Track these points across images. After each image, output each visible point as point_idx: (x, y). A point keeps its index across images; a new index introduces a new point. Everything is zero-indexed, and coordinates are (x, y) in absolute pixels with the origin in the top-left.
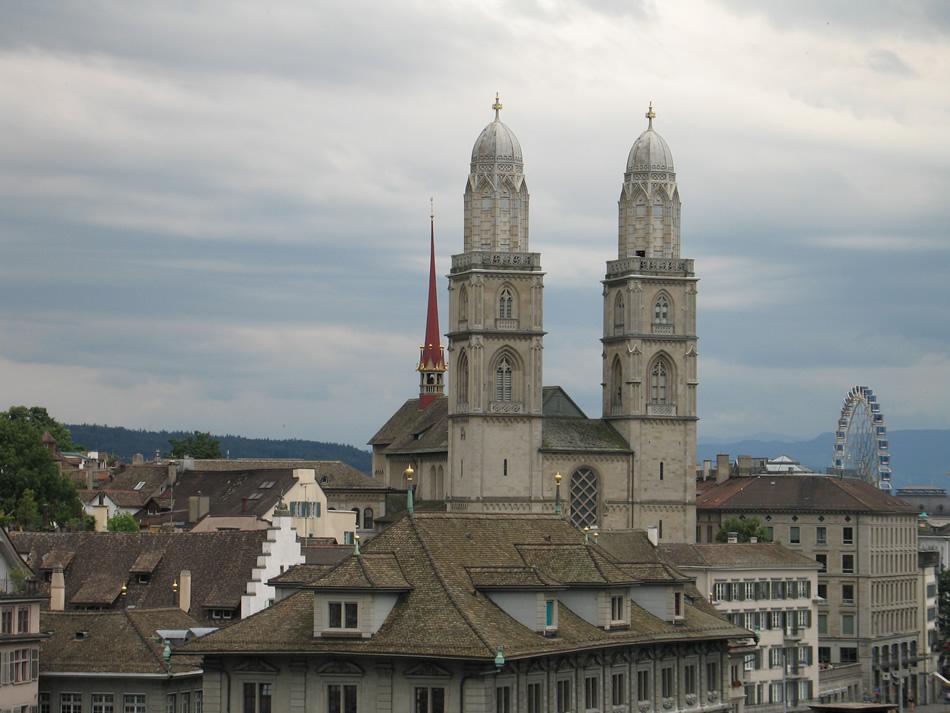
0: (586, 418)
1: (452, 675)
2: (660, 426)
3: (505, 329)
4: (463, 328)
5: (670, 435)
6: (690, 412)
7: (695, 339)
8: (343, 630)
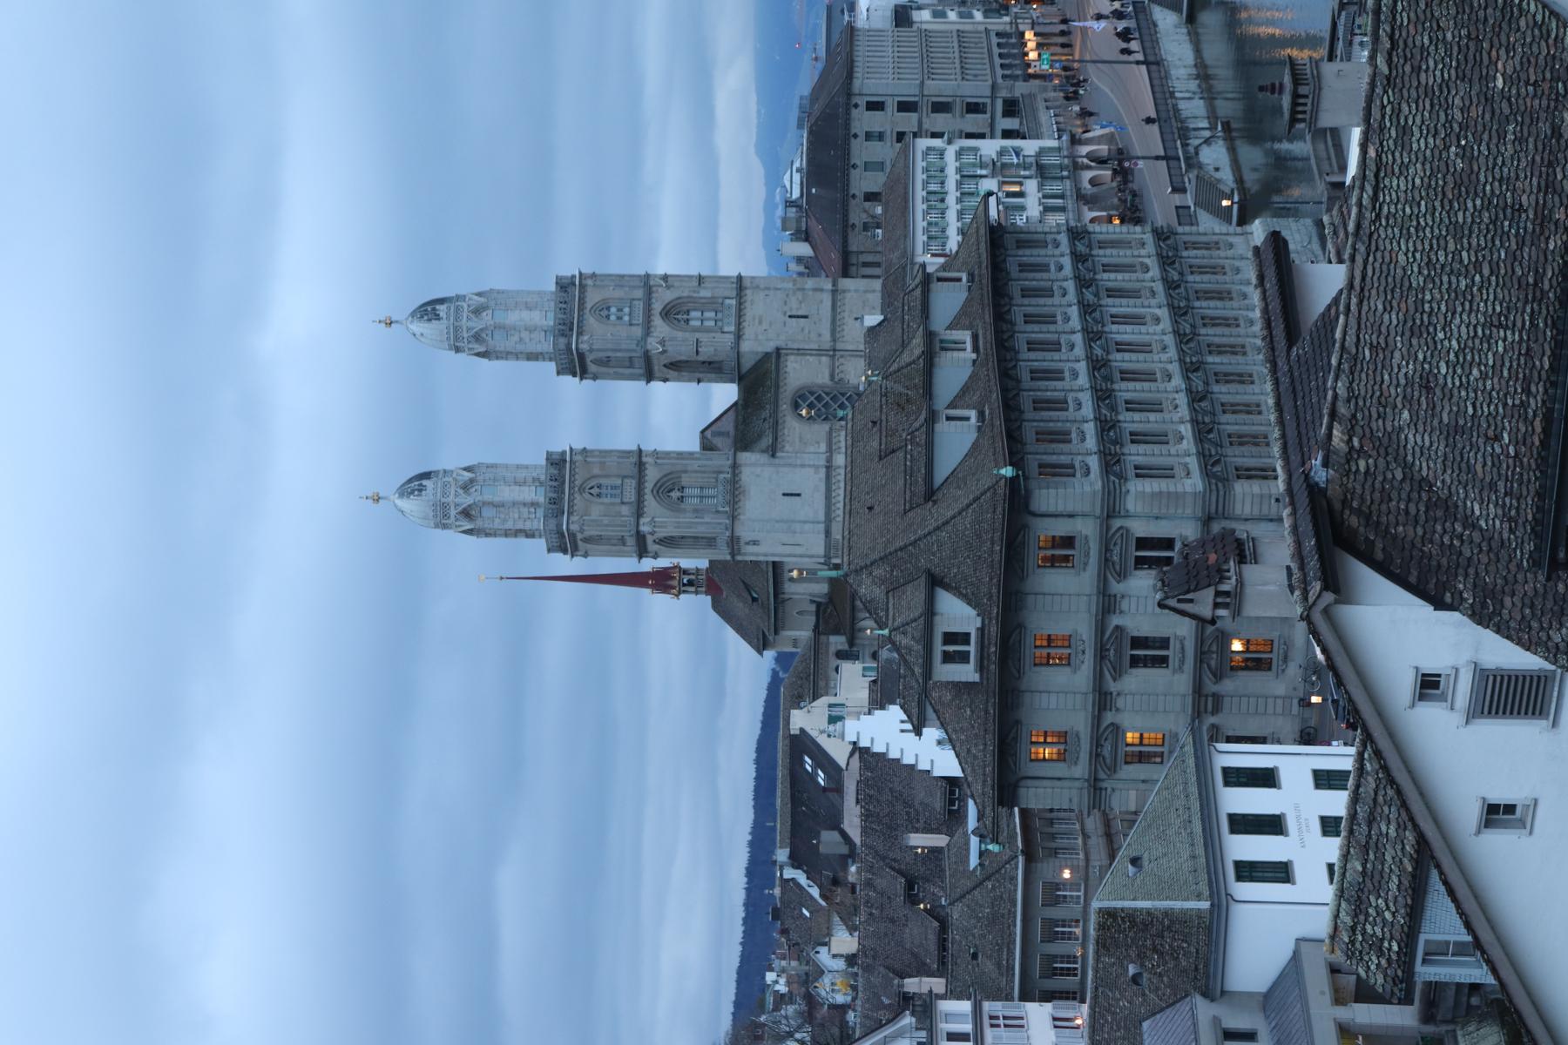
0: (735, 404)
1: (1025, 527)
4: (631, 541)
5: (757, 306)
8: (972, 648)
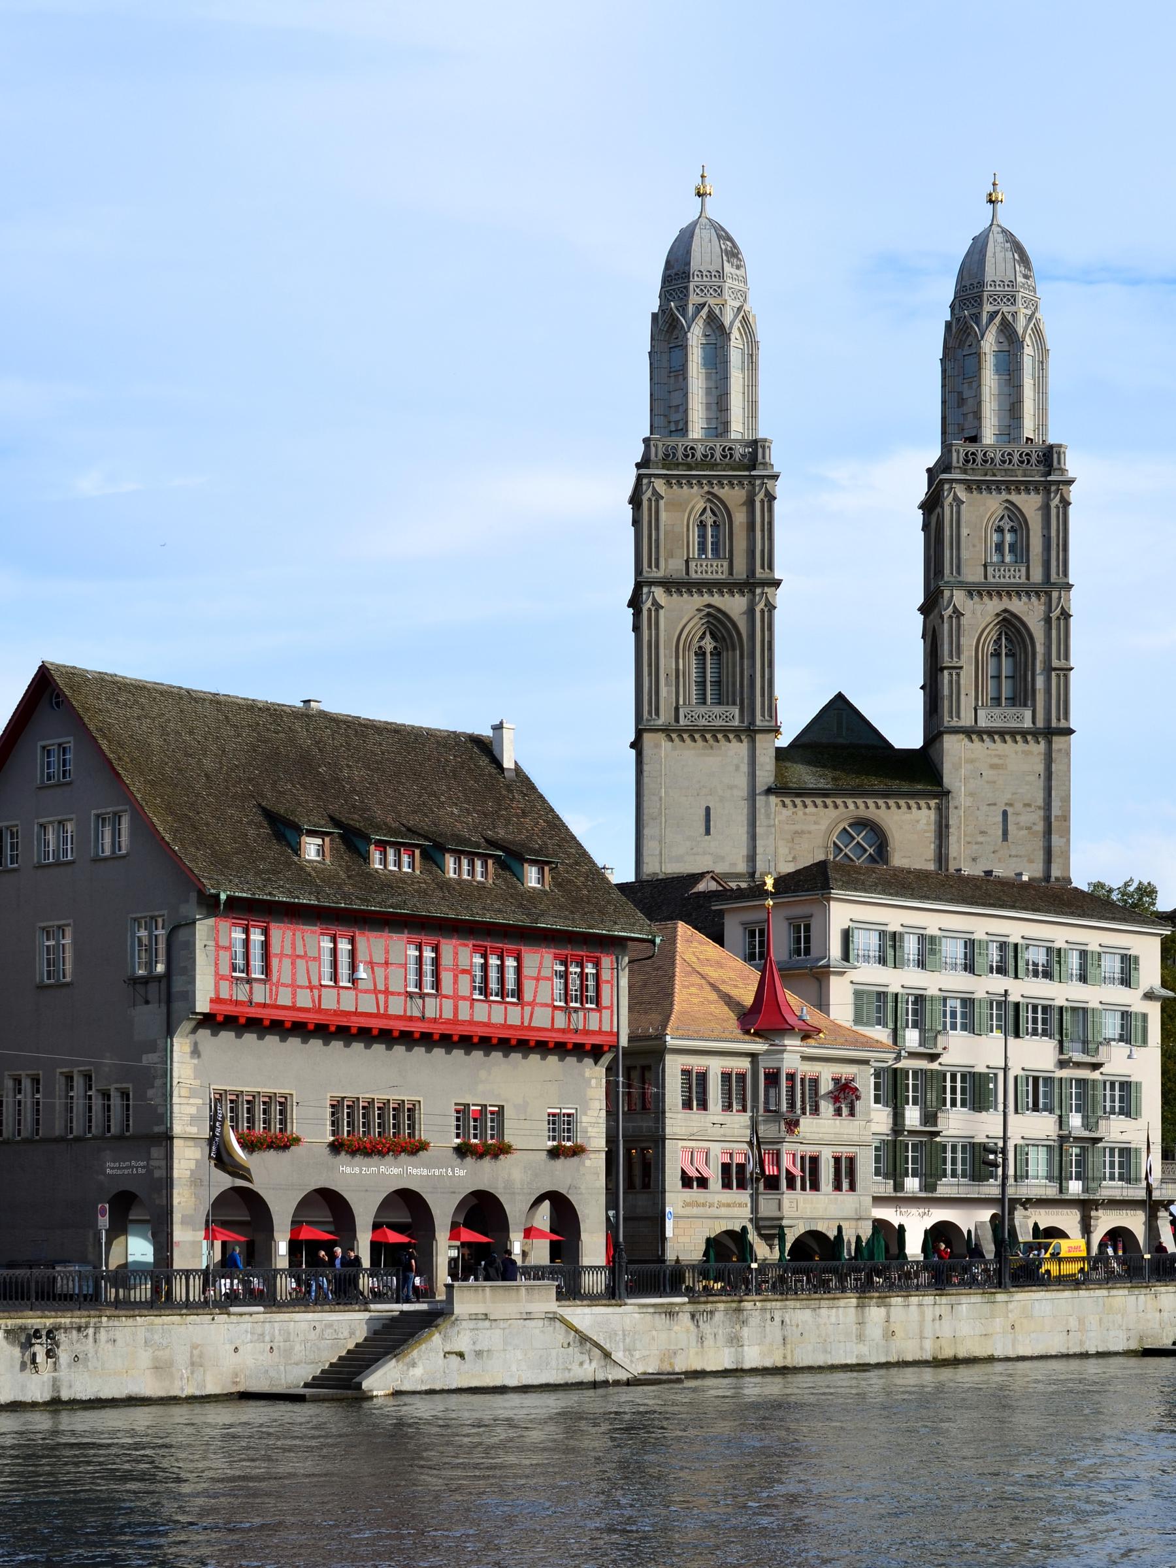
0: (890, 746)
2: (999, 745)
3: (709, 576)
5: (1023, 759)
6: (1059, 720)
7: (1069, 587)
